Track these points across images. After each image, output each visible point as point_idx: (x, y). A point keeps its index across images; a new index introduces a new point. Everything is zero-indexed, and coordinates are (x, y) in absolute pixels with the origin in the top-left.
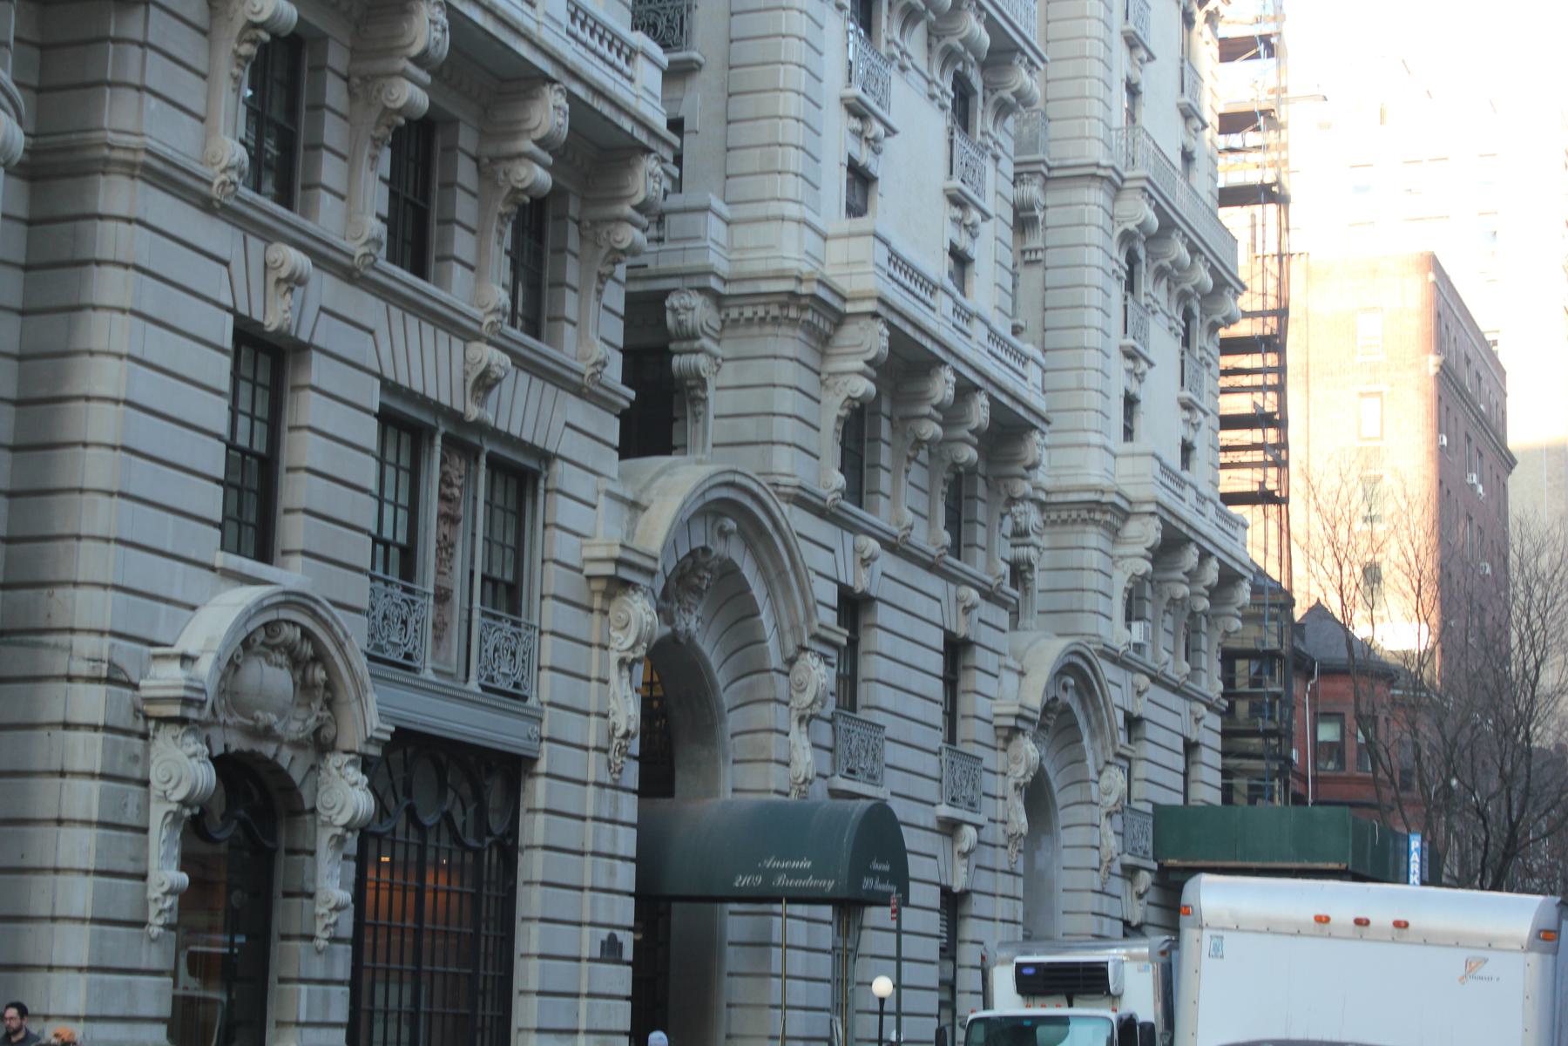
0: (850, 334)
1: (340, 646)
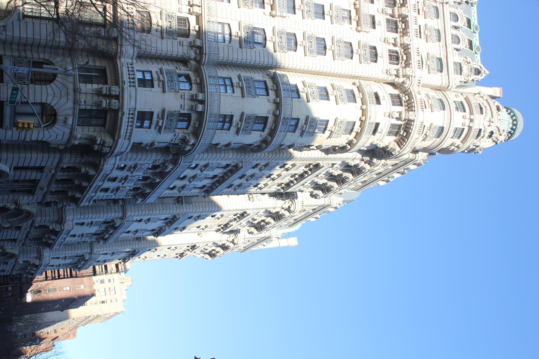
0: (58, 226)
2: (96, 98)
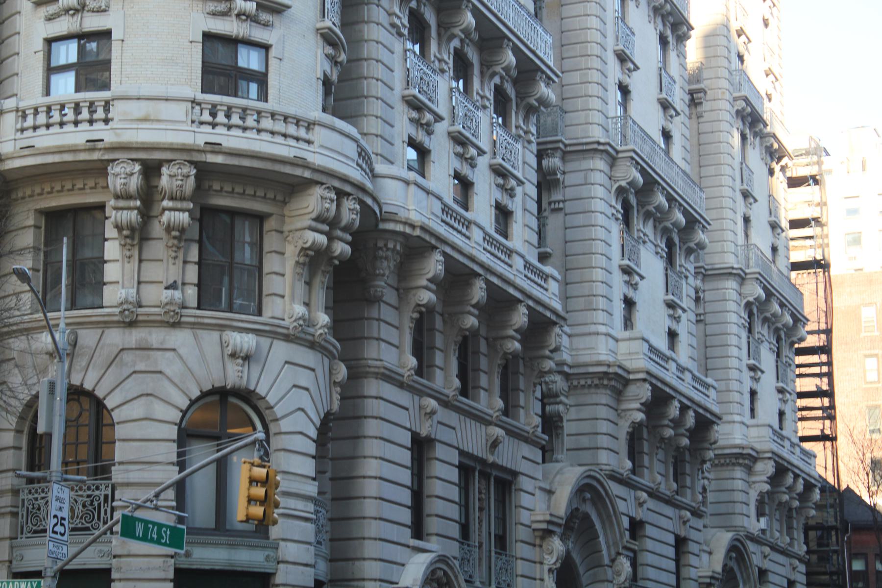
0: (632, 390)
2: (158, 248)
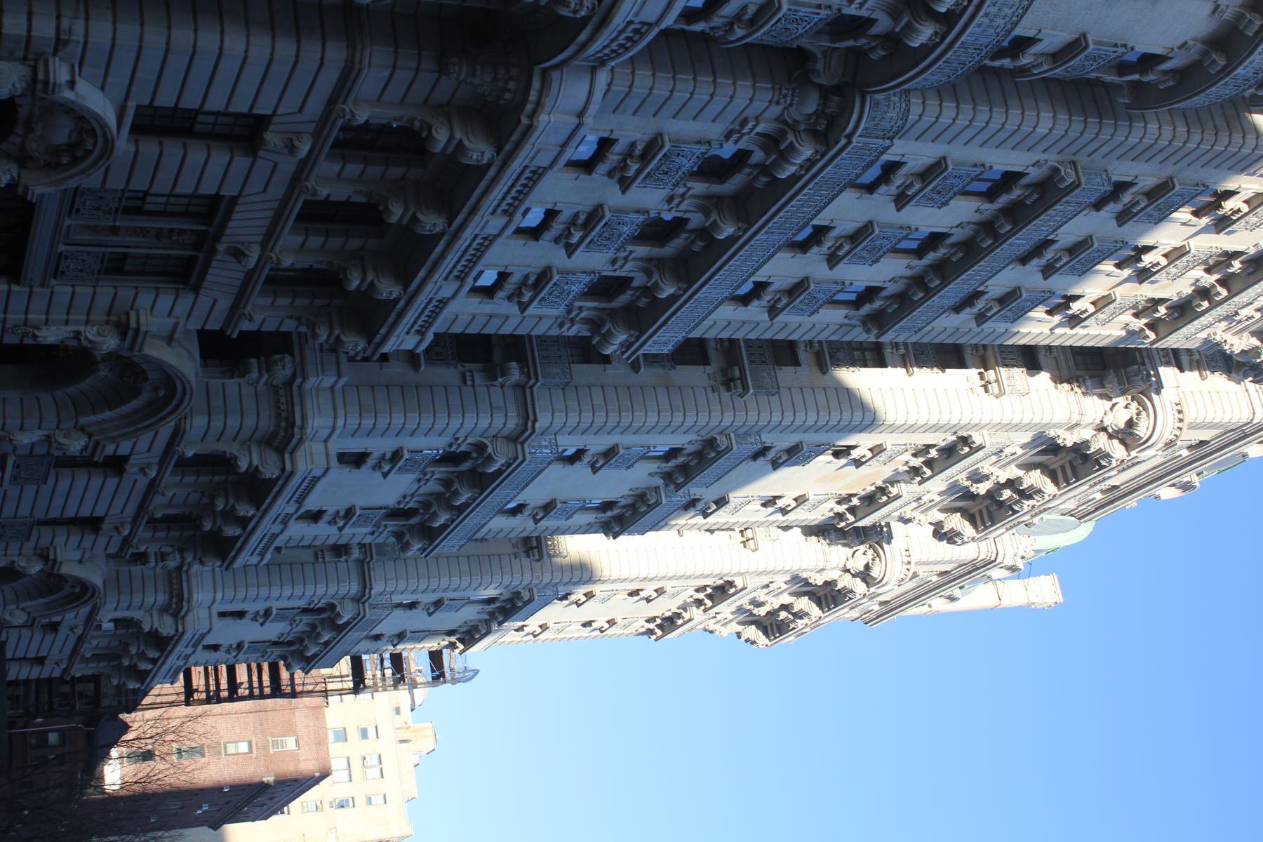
0: (272, 457)
1: (82, 172)
